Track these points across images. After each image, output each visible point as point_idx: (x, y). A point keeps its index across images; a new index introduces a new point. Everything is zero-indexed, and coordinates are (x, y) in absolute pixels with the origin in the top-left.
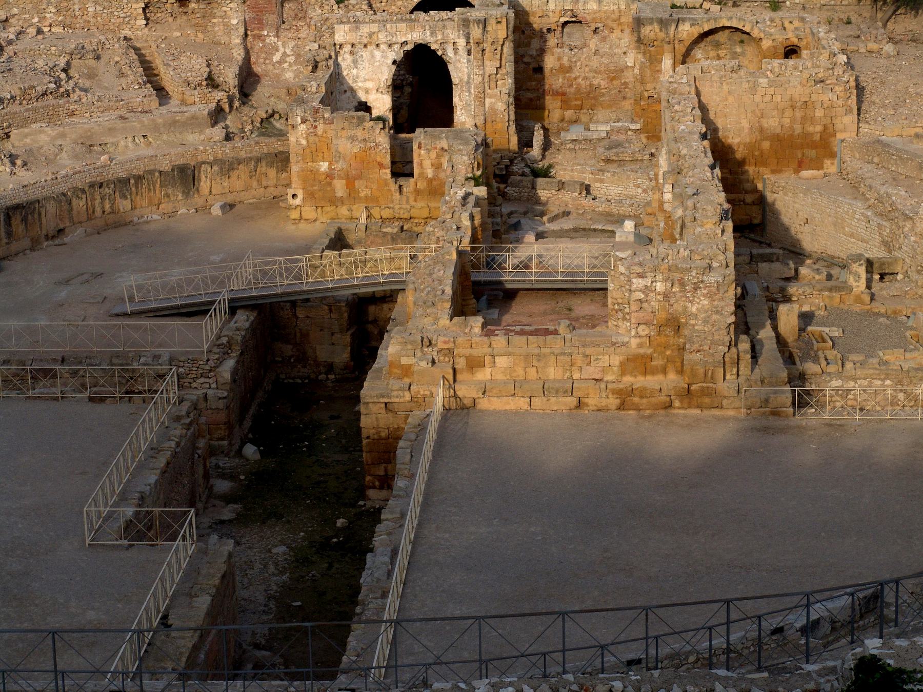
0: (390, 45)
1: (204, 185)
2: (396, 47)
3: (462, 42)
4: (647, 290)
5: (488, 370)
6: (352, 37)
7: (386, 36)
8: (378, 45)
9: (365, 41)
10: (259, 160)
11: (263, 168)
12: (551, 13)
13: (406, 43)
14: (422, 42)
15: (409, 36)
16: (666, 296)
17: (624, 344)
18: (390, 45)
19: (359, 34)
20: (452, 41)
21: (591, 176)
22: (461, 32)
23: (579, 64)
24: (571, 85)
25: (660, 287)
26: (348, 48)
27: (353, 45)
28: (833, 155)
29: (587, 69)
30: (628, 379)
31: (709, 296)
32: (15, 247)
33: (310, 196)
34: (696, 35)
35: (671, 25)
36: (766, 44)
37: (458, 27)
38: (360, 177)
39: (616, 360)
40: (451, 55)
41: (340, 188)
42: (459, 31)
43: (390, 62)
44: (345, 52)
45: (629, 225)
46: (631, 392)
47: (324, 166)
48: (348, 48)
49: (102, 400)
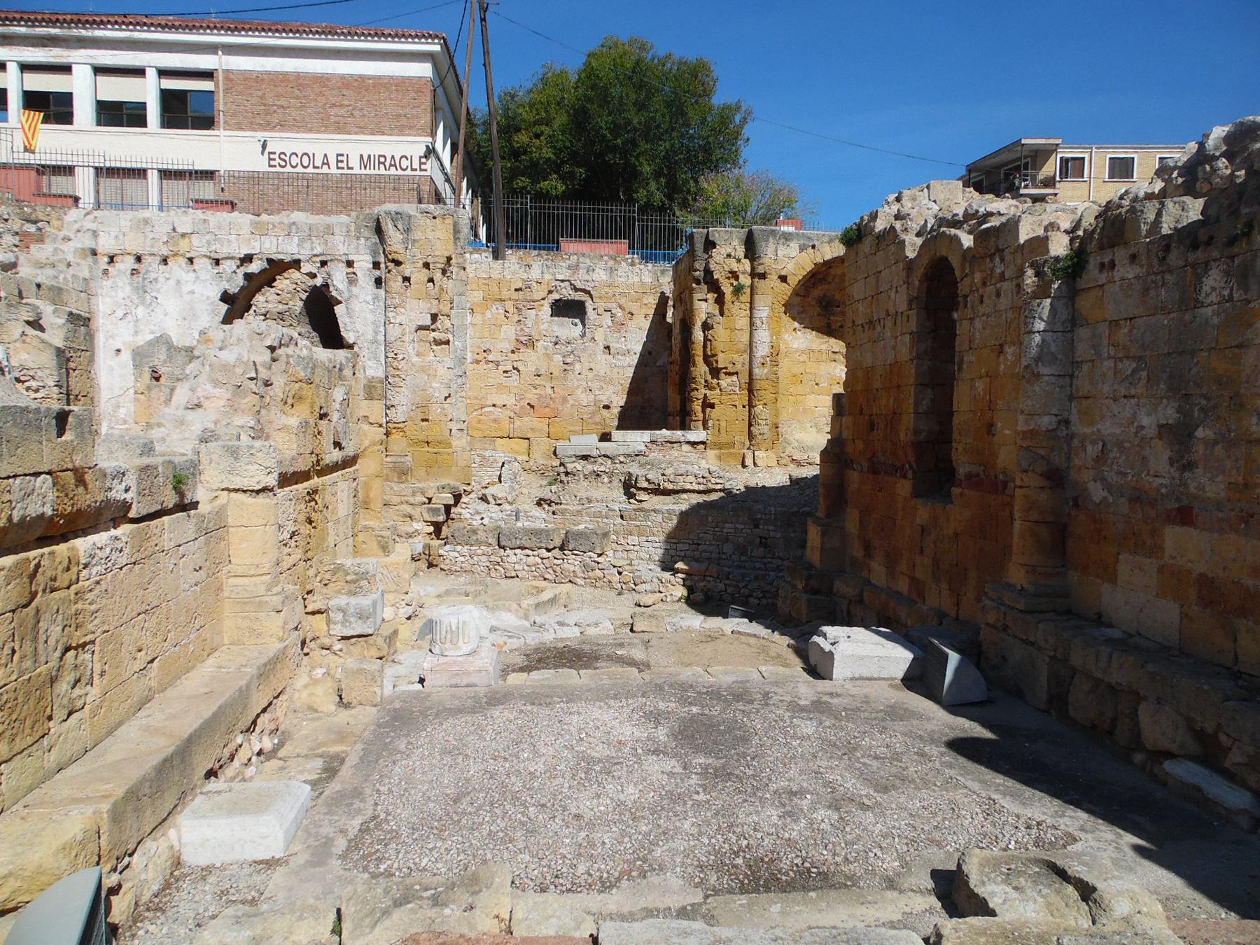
0: (217, 262)
2: (228, 266)
3: (363, 263)
6: (135, 244)
7: (208, 243)
8: (191, 260)
9: (165, 251)
12: (534, 284)
13: (248, 259)
14: (280, 257)
15: (257, 244)
18: (217, 262)
19: (151, 235)
20: (344, 258)
21: (619, 521)
22: (363, 240)
23: (578, 366)
24: (565, 400)
26: (127, 264)
27: (139, 259)
29: (591, 375)
34: (809, 267)
35: (767, 241)
37: (358, 229)
40: (340, 286)
42: (358, 239)
43: (216, 293)
44: (118, 271)
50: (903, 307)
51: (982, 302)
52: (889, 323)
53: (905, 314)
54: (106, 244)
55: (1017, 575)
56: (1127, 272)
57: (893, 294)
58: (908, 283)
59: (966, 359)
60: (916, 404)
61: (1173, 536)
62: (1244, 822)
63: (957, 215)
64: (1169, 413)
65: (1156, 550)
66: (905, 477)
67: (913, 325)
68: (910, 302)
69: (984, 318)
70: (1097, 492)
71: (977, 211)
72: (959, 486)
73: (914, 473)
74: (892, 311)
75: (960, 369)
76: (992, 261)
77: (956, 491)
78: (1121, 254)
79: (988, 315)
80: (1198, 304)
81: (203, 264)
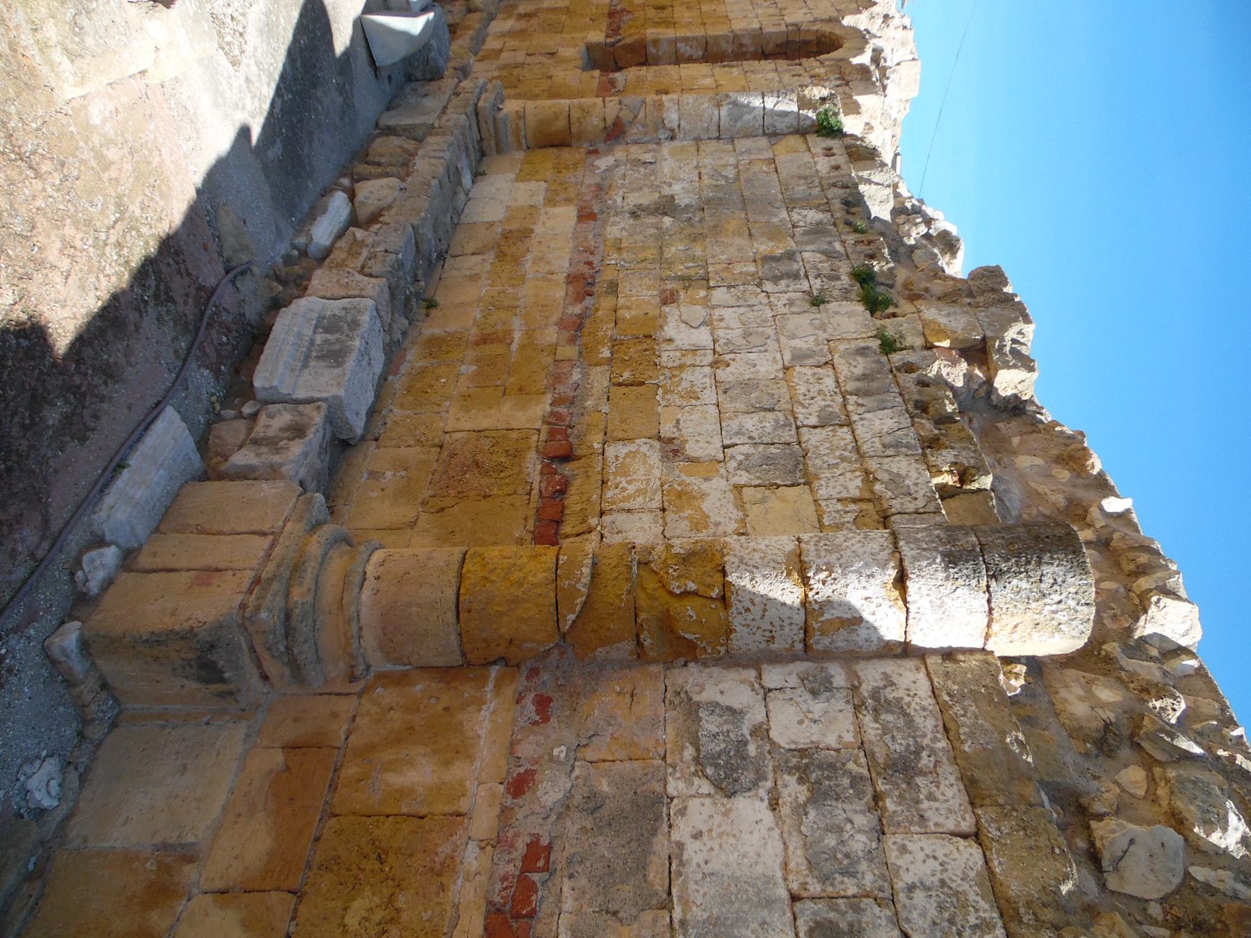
50: (788, 19)
51: (794, 76)
52: (772, 11)
53: (783, 22)
55: (511, 106)
56: (823, 165)
57: (803, 11)
58: (815, 20)
59: (734, 70)
60: (686, 40)
61: (565, 215)
62: (301, 240)
63: (885, 61)
64: (683, 200)
65: (551, 201)
66: (607, 36)
67: (769, 29)
68: (795, 25)
69: (777, 79)
70: (603, 163)
71: (888, 78)
72: (601, 75)
73: (613, 44)
74: (784, 12)
75: (725, 66)
76: (837, 79)
77: (597, 73)
78: (841, 159)
79: (780, 81)
80: (789, 209)
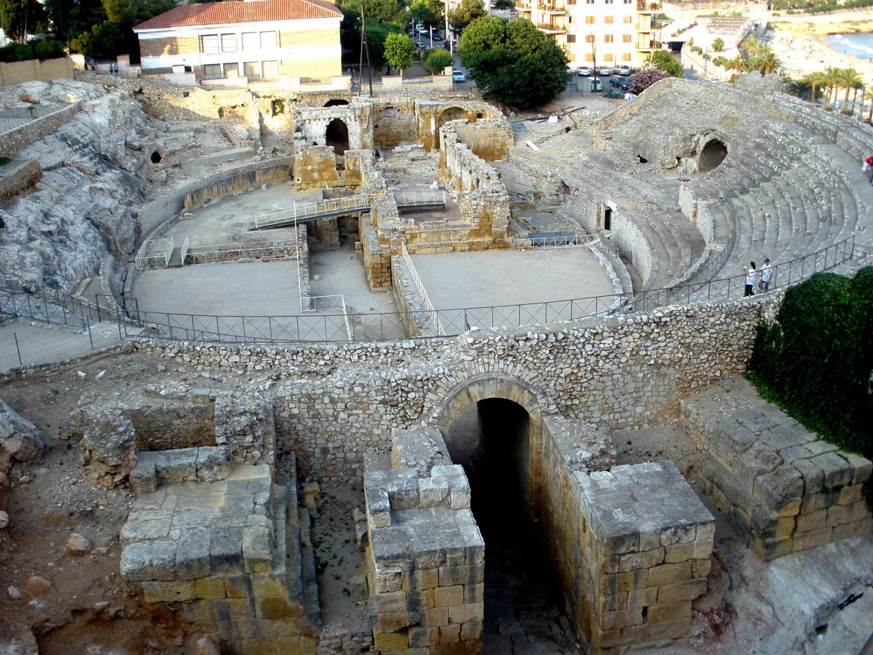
1: (258, 178)
3: (353, 117)
4: (477, 205)
5: (418, 239)
10: (277, 167)
11: (278, 170)
16: (485, 207)
17: (470, 226)
25: (482, 203)
28: (505, 154)
30: (471, 240)
31: (501, 206)
32: (195, 207)
33: (304, 179)
36: (470, 113)
38: (324, 170)
39: (467, 232)
41: (316, 175)
45: (435, 183)
46: (473, 243)
47: (310, 167)
48: (307, 122)
49: (268, 261)
54: (304, 118)
81: (322, 120)
